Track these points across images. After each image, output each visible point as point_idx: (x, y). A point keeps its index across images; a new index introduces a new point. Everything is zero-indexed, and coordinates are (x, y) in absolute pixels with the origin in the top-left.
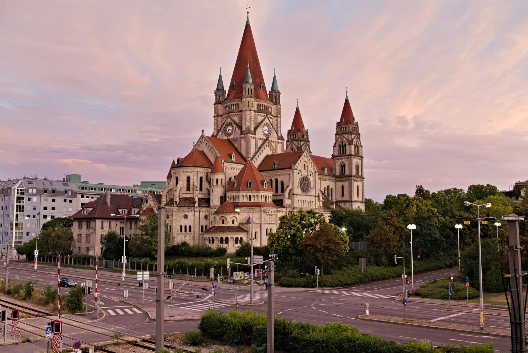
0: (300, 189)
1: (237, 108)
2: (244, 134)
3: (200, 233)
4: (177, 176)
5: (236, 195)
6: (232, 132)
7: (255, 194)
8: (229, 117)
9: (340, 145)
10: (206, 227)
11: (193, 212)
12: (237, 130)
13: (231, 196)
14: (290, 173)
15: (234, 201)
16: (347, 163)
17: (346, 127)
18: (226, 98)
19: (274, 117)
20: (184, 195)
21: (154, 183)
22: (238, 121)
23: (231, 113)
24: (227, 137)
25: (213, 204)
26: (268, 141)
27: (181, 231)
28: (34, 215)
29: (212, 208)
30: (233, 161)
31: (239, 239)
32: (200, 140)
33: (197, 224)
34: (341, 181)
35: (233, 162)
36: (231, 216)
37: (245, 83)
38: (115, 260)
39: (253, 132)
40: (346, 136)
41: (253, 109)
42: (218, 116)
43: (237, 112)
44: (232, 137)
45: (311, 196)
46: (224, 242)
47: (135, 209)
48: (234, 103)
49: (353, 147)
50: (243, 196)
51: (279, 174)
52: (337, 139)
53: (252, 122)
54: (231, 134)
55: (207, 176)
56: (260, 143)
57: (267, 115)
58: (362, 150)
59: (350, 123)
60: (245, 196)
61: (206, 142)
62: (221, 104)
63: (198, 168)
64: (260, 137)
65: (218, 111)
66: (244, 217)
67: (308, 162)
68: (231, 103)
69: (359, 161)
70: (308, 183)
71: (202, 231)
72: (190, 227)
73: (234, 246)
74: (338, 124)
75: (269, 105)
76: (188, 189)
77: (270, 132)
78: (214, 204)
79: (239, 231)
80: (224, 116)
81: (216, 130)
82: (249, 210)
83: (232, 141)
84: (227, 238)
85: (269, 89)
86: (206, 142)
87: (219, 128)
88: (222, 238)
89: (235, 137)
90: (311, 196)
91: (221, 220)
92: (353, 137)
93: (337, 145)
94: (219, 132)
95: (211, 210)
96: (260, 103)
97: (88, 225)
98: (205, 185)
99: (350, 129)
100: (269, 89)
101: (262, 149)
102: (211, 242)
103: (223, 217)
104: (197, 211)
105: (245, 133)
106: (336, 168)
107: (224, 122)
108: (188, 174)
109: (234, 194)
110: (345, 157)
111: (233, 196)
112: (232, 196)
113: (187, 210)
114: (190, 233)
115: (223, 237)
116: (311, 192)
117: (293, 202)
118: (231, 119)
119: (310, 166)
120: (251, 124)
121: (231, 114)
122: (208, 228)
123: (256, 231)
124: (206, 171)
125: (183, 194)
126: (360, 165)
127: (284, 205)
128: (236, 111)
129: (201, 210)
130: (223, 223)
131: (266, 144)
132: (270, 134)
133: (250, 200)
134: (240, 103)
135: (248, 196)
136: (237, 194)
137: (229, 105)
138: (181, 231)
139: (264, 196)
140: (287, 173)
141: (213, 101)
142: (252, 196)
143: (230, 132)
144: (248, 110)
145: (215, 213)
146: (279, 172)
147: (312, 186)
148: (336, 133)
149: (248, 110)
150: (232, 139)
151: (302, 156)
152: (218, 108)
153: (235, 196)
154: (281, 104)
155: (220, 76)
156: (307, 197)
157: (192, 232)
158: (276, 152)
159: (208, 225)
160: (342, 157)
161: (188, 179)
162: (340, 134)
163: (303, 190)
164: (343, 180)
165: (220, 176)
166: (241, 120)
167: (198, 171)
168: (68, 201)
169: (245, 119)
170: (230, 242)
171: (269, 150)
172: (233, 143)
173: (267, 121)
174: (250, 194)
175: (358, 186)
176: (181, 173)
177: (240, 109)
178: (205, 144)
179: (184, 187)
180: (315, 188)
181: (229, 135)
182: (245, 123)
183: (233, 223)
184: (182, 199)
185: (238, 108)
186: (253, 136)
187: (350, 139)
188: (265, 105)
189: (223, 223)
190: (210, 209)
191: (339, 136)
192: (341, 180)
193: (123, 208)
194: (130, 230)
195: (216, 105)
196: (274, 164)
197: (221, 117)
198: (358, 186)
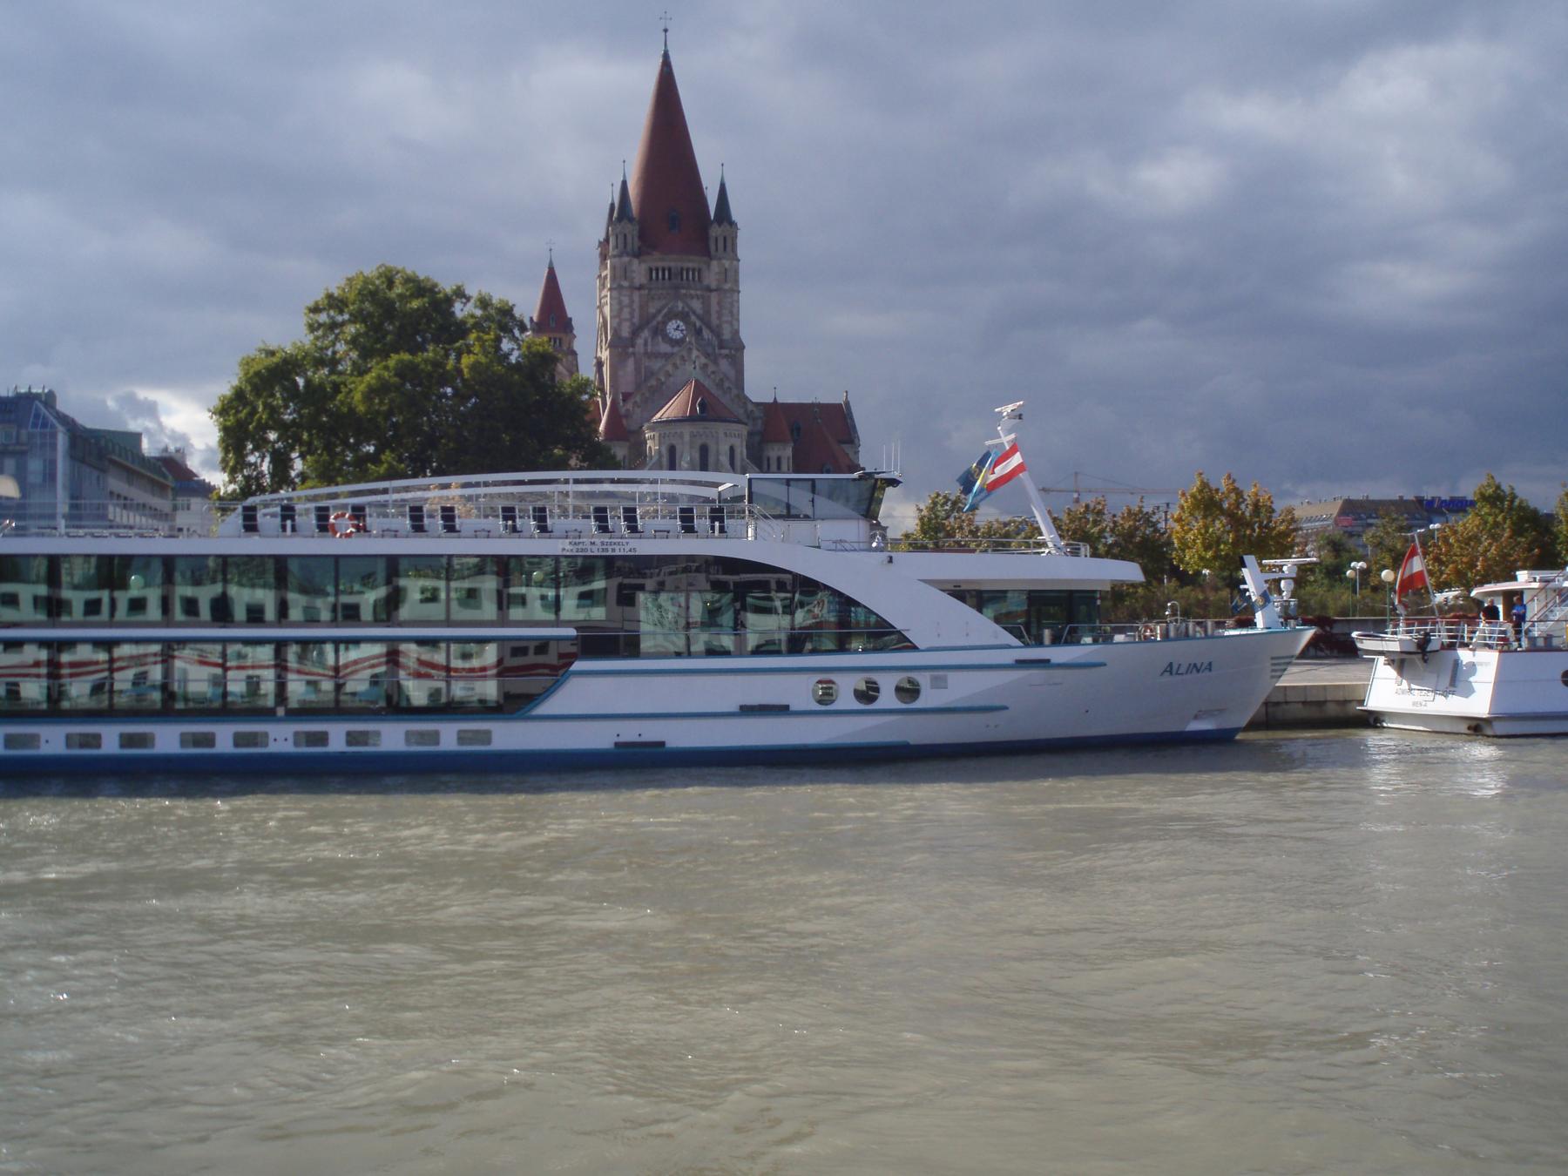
1: (697, 278)
12: (706, 334)
24: (673, 346)
37: (725, 224)
42: (633, 288)
48: (690, 265)
68: (679, 264)
87: (636, 320)
118: (688, 306)
121: (683, 291)
143: (677, 335)
161: (732, 449)
166: (707, 311)
176: (721, 435)
177: (706, 282)
195: (626, 259)
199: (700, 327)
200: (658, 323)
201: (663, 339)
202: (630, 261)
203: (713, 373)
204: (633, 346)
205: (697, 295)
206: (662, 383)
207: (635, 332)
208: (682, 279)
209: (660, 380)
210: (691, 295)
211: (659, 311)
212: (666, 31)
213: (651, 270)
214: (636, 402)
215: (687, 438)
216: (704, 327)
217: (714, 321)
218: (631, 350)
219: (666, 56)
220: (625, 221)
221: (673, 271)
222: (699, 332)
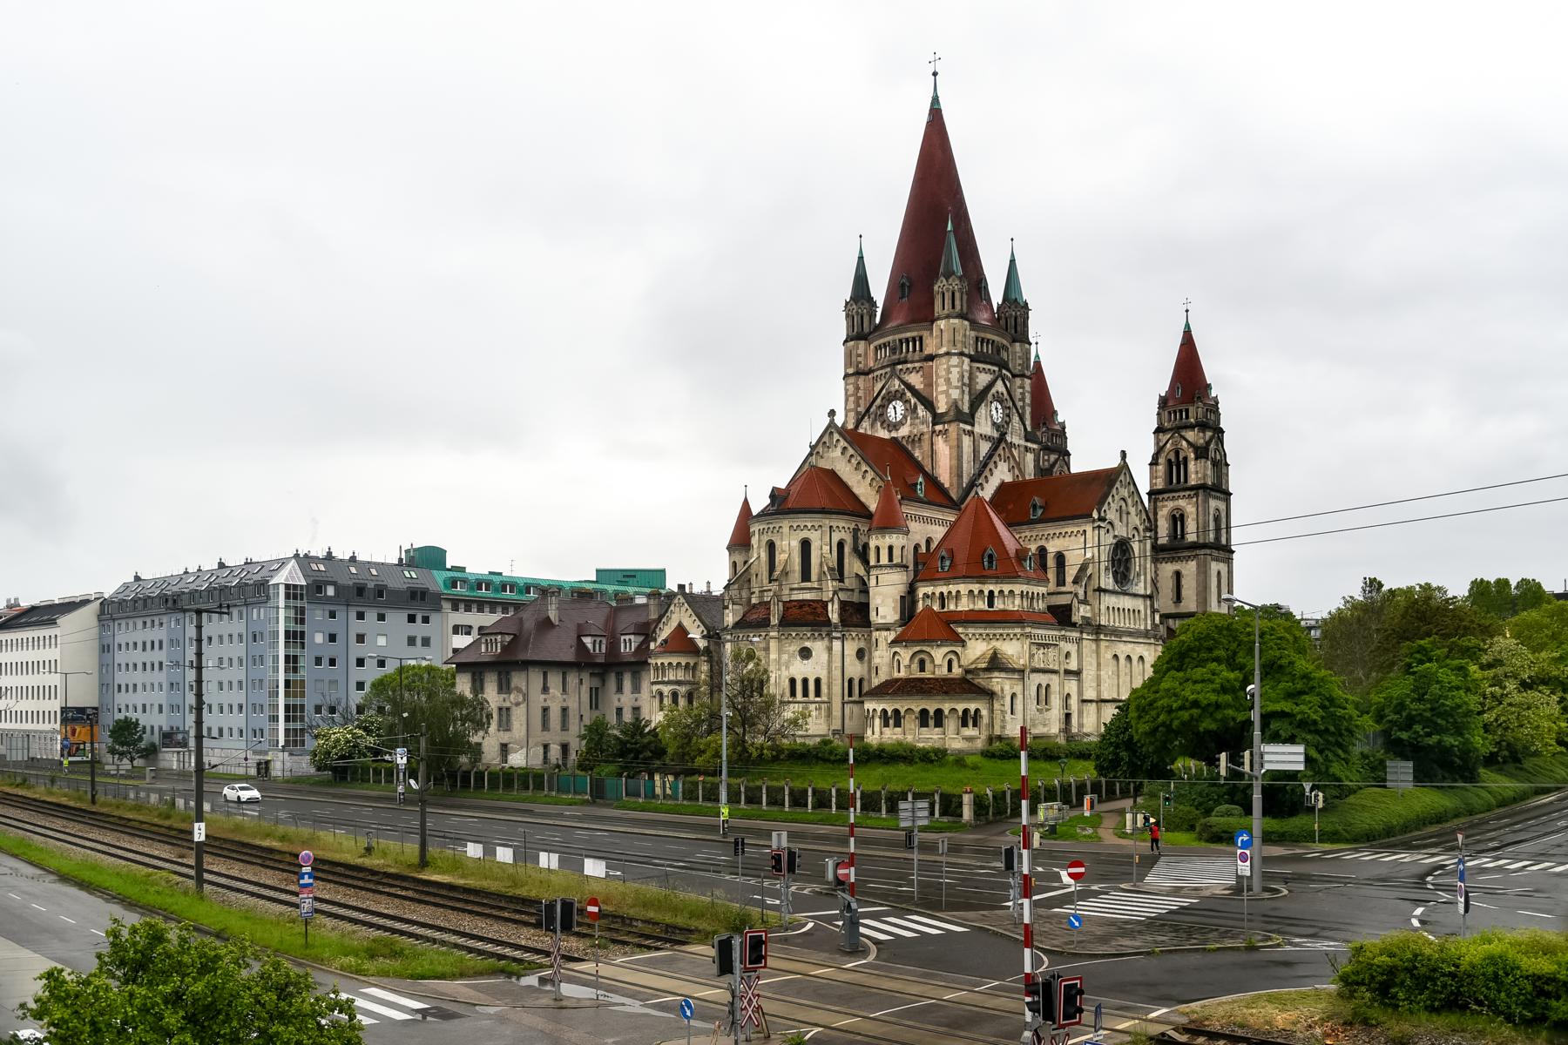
0: (1111, 575)
2: (944, 423)
3: (846, 698)
5: (950, 592)
6: (905, 417)
7: (1006, 588)
8: (893, 374)
9: (1169, 461)
10: (861, 681)
11: (826, 642)
12: (920, 409)
13: (933, 593)
14: (1085, 531)
15: (943, 608)
16: (1189, 507)
17: (1187, 411)
18: (878, 320)
19: (1014, 376)
22: (922, 386)
23: (899, 363)
24: (890, 431)
25: (880, 621)
26: (1003, 445)
27: (793, 693)
28: (432, 641)
29: (877, 630)
30: (920, 498)
31: (972, 713)
32: (824, 440)
33: (837, 673)
34: (1173, 560)
35: (920, 501)
36: (946, 649)
38: (628, 777)
40: (1191, 435)
41: (966, 351)
42: (858, 373)
44: (904, 431)
45: (1135, 595)
46: (931, 722)
47: (632, 637)
48: (908, 335)
51: (1052, 532)
52: (1161, 444)
53: (966, 389)
54: (901, 423)
55: (855, 538)
57: (1000, 370)
58: (1227, 475)
59: (1199, 398)
60: (976, 592)
61: (843, 443)
62: (866, 339)
63: (834, 516)
64: (984, 433)
65: (860, 359)
66: (978, 653)
67: (1129, 501)
68: (898, 337)
69: (1222, 506)
70: (1128, 560)
71: (850, 695)
72: (818, 681)
74: (1163, 402)
75: (1005, 342)
76: (806, 576)
77: (1008, 419)
78: (884, 617)
79: (970, 691)
80: (879, 373)
81: (852, 414)
83: (904, 443)
84: (939, 712)
85: (997, 296)
87: (862, 409)
90: (1135, 595)
91: (916, 660)
92: (1207, 438)
93: (1161, 460)
95: (875, 634)
96: (982, 335)
97: (504, 680)
98: (853, 566)
100: (997, 296)
101: (991, 465)
102: (891, 722)
104: (836, 638)
105: (947, 419)
106: (1159, 523)
107: (877, 389)
109: (945, 589)
110: (1187, 493)
111: (942, 594)
112: (937, 595)
114: (818, 699)
115: (927, 707)
116: (1136, 585)
119: (1133, 510)
120: (963, 392)
121: (900, 367)
122: (865, 684)
123: (1014, 691)
124: (852, 526)
125: (792, 589)
126: (1223, 515)
128: (917, 358)
129: (847, 634)
130: (922, 669)
131: (998, 452)
132: (1008, 424)
133: (991, 604)
134: (925, 334)
135: (986, 593)
136: (953, 588)
137: (894, 341)
138: (793, 693)
139: (1028, 593)
140: (1075, 529)
141: (842, 331)
142: (996, 594)
144: (955, 354)
145: (895, 642)
146: (1051, 529)
147: (1137, 569)
149: (955, 354)
150: (903, 437)
151: (1118, 485)
152: (859, 352)
156: (1127, 597)
157: (824, 698)
158: (1023, 475)
159: (866, 677)
160: (1177, 494)
161: (806, 545)
163: (1116, 581)
164: (1179, 558)
165: (895, 540)
166: (929, 384)
167: (834, 524)
169: (948, 381)
170: (946, 722)
171: (1006, 469)
173: (999, 387)
175: (1219, 573)
176: (786, 530)
177: (928, 351)
178: (839, 450)
179: (794, 571)
180: (1145, 574)
181: (895, 426)
183: (950, 670)
184: (788, 605)
185: (921, 350)
186: (968, 428)
187: (1202, 441)
188: (993, 341)
189: (922, 669)
190: (871, 632)
192: (1173, 558)
194: (618, 696)
196: (1035, 507)
198: (1219, 573)
199: (915, 404)
200: (879, 407)
201: (882, 425)
203: (852, 456)
210: (908, 369)
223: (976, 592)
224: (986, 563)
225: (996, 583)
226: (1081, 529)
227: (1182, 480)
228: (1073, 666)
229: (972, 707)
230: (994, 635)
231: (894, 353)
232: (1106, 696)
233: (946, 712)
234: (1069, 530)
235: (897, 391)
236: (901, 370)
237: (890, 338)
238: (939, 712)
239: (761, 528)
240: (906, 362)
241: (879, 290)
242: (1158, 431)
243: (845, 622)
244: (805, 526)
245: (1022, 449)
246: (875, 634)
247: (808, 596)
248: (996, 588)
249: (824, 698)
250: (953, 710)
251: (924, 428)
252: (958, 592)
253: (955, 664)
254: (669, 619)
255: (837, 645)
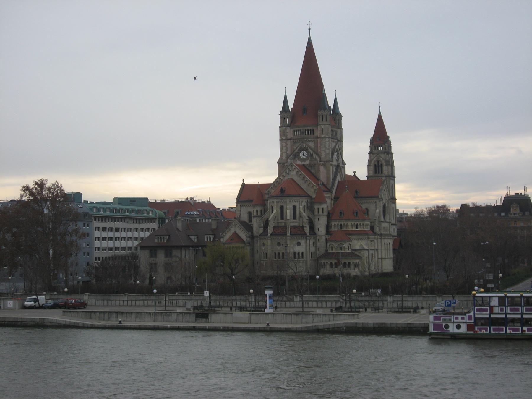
1: (312, 133)
4: (283, 205)
5: (344, 224)
6: (307, 158)
7: (362, 223)
9: (375, 165)
10: (314, 252)
11: (305, 239)
12: (315, 156)
13: (338, 224)
14: (376, 202)
20: (292, 223)
21: (135, 200)
22: (314, 147)
23: (306, 138)
36: (348, 243)
39: (331, 160)
40: (383, 156)
42: (287, 139)
43: (312, 138)
44: (307, 163)
45: (387, 222)
46: (347, 266)
48: (309, 128)
49: (390, 166)
50: (350, 226)
53: (330, 149)
56: (334, 168)
57: (337, 141)
60: (353, 224)
62: (290, 127)
65: (287, 134)
67: (386, 190)
68: (304, 128)
72: (302, 253)
73: (354, 270)
76: (295, 218)
77: (338, 157)
78: (321, 232)
82: (359, 237)
83: (308, 167)
84: (349, 263)
86: (296, 170)
88: (331, 263)
89: (312, 163)
90: (387, 222)
94: (290, 156)
99: (387, 148)
102: (334, 266)
103: (341, 244)
108: (294, 204)
109: (342, 223)
111: (341, 225)
112: (339, 225)
113: (300, 238)
117: (380, 229)
119: (386, 193)
121: (306, 139)
124: (306, 200)
127: (375, 231)
133: (357, 228)
134: (315, 129)
135: (356, 225)
137: (303, 130)
140: (372, 201)
142: (359, 225)
148: (369, 151)
149: (328, 137)
150: (307, 165)
152: (287, 131)
153: (343, 225)
154: (343, 126)
155: (285, 97)
157: (305, 259)
161: (294, 207)
162: (376, 153)
166: (317, 147)
167: (303, 200)
168: (86, 225)
169: (325, 147)
172: (310, 168)
173: (337, 147)
174: (357, 223)
176: (288, 202)
182: (325, 151)
185: (313, 134)
187: (387, 158)
191: (375, 155)
193: (208, 235)
197: (289, 141)
199: (312, 153)
200: (296, 153)
201: (298, 159)
202: (285, 129)
203: (300, 175)
204: (286, 163)
205: (311, 140)
206: (282, 180)
207: (287, 158)
208: (306, 134)
209: (281, 178)
210: (309, 140)
211: (297, 148)
212: (309, 29)
213: (294, 131)
214: (271, 188)
215: (275, 203)
216: (314, 153)
217: (319, 151)
218: (286, 164)
219: (309, 39)
220: (284, 113)
221: (302, 131)
222: (312, 155)
223: (353, 224)
224: (355, 214)
225: (358, 221)
226: (375, 201)
227: (380, 172)
228: (376, 248)
229: (358, 261)
230: (360, 238)
231: (303, 134)
232: (383, 257)
233: (351, 263)
234: (370, 201)
235: (304, 148)
236: (306, 140)
237: (301, 128)
238: (349, 263)
239: (278, 200)
240: (307, 138)
241: (291, 106)
242: (369, 153)
243: (310, 234)
244: (295, 201)
245: (342, 167)
246: (318, 237)
247: (296, 224)
248: (359, 223)
249: (305, 259)
250: (353, 262)
251: (316, 162)
252: (347, 224)
253: (350, 247)
254: (230, 230)
255: (308, 241)
